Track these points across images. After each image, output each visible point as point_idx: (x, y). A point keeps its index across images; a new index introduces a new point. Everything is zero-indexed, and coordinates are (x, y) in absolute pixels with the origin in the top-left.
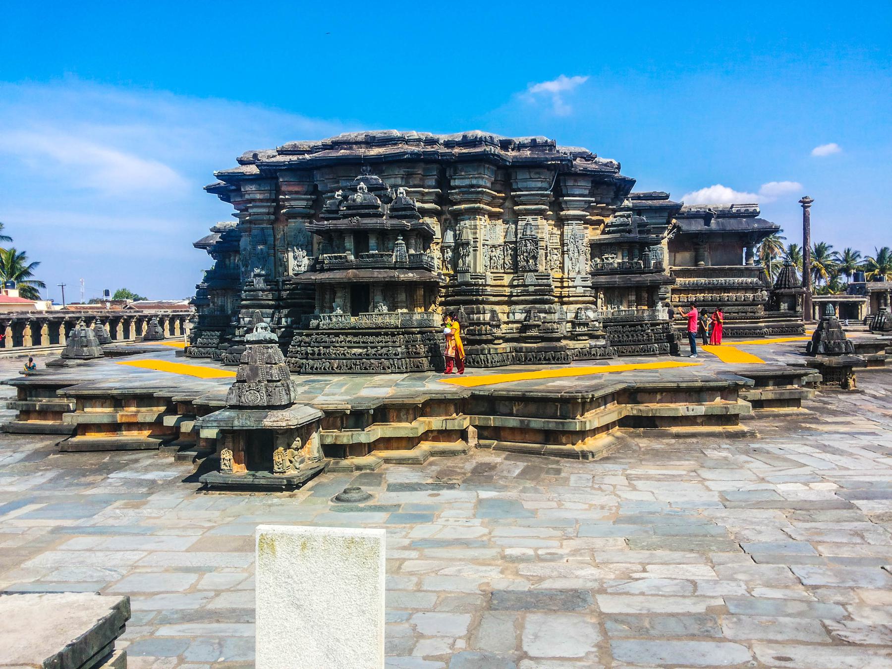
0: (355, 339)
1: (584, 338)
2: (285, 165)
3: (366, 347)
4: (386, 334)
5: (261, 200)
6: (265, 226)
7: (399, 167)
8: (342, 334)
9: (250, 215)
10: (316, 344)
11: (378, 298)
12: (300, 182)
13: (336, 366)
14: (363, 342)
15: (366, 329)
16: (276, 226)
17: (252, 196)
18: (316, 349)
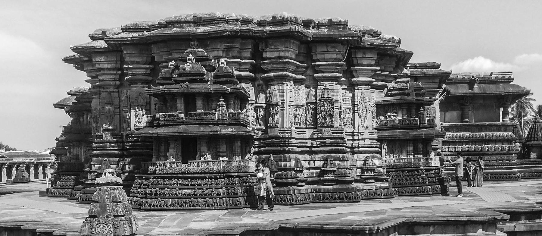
0: (185, 182)
1: (371, 181)
2: (128, 41)
3: (194, 189)
4: (210, 178)
5: (109, 69)
6: (111, 90)
7: (221, 42)
8: (175, 178)
9: (100, 81)
10: (153, 186)
11: (204, 148)
12: (140, 54)
13: (169, 204)
14: (192, 185)
15: (194, 173)
16: (120, 90)
17: (101, 66)
18: (153, 190)
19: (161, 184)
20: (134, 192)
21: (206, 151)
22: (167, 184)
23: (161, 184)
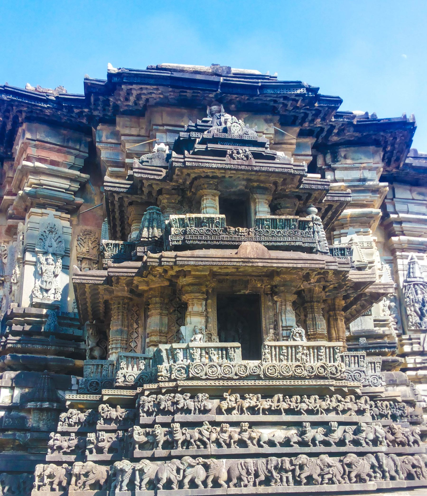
2: (47, 101)
10: (160, 418)
11: (289, 318)
19: (188, 411)
20: (60, 448)
21: (294, 324)
22: (205, 411)
23: (188, 411)
